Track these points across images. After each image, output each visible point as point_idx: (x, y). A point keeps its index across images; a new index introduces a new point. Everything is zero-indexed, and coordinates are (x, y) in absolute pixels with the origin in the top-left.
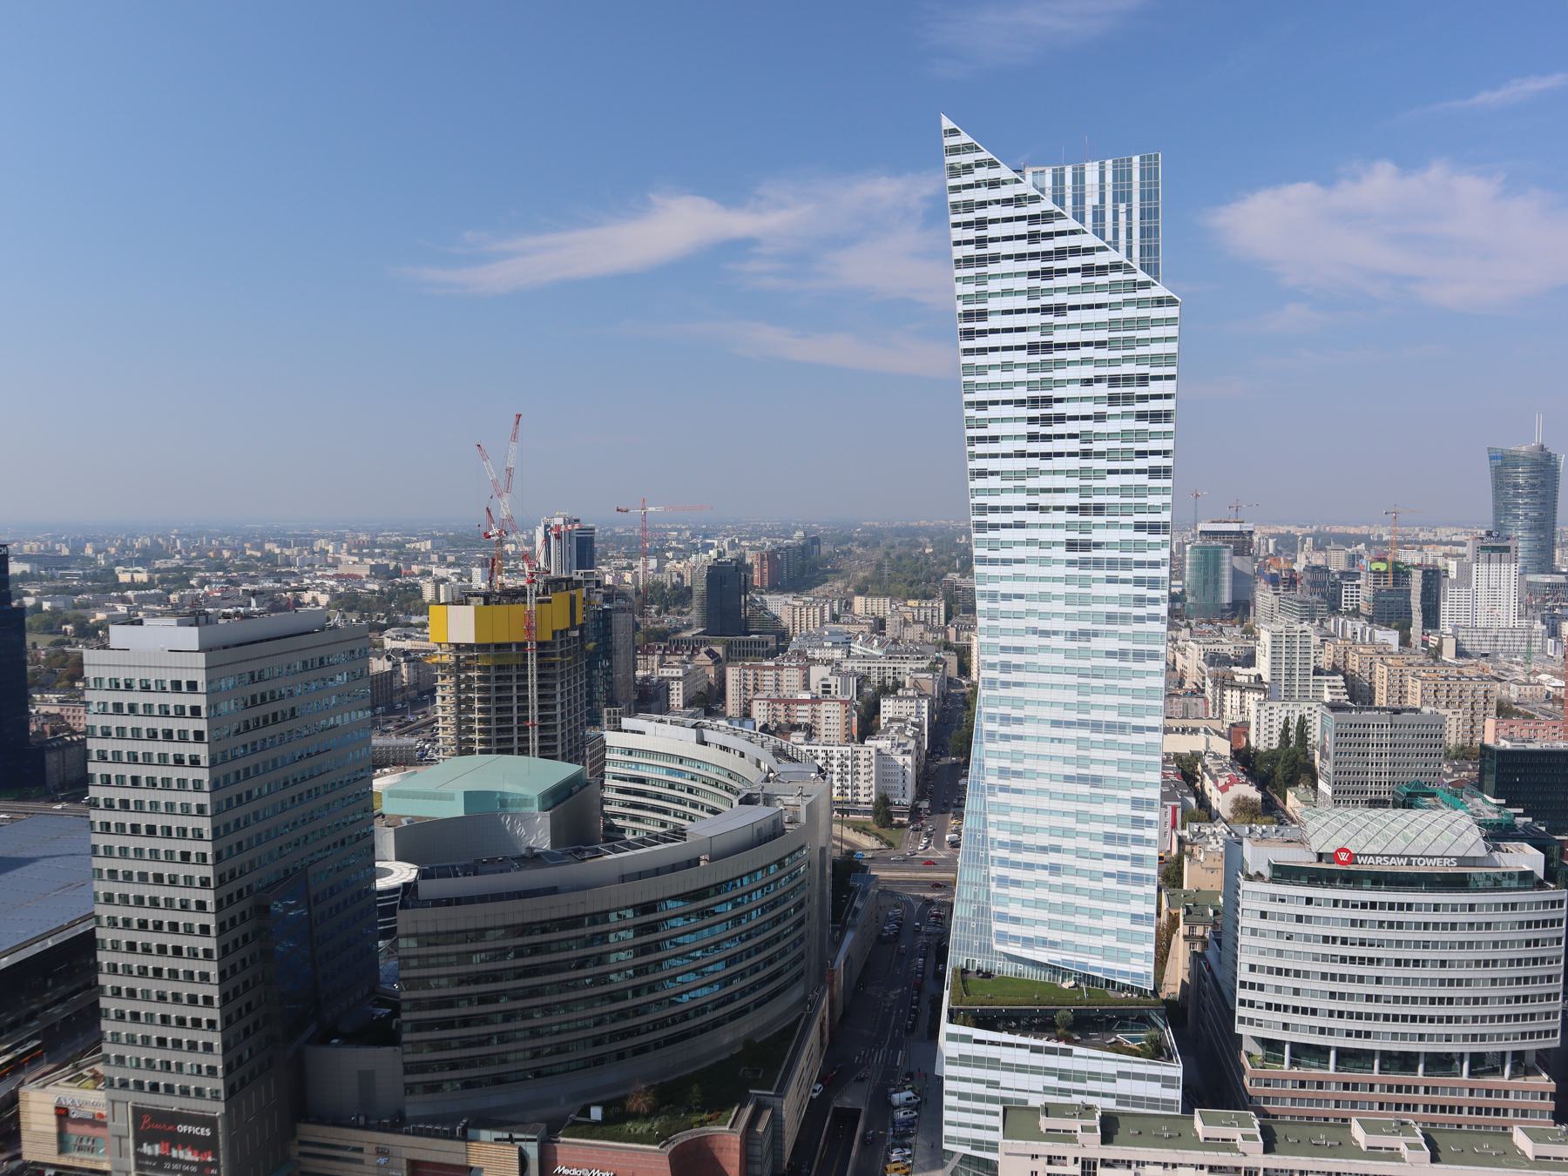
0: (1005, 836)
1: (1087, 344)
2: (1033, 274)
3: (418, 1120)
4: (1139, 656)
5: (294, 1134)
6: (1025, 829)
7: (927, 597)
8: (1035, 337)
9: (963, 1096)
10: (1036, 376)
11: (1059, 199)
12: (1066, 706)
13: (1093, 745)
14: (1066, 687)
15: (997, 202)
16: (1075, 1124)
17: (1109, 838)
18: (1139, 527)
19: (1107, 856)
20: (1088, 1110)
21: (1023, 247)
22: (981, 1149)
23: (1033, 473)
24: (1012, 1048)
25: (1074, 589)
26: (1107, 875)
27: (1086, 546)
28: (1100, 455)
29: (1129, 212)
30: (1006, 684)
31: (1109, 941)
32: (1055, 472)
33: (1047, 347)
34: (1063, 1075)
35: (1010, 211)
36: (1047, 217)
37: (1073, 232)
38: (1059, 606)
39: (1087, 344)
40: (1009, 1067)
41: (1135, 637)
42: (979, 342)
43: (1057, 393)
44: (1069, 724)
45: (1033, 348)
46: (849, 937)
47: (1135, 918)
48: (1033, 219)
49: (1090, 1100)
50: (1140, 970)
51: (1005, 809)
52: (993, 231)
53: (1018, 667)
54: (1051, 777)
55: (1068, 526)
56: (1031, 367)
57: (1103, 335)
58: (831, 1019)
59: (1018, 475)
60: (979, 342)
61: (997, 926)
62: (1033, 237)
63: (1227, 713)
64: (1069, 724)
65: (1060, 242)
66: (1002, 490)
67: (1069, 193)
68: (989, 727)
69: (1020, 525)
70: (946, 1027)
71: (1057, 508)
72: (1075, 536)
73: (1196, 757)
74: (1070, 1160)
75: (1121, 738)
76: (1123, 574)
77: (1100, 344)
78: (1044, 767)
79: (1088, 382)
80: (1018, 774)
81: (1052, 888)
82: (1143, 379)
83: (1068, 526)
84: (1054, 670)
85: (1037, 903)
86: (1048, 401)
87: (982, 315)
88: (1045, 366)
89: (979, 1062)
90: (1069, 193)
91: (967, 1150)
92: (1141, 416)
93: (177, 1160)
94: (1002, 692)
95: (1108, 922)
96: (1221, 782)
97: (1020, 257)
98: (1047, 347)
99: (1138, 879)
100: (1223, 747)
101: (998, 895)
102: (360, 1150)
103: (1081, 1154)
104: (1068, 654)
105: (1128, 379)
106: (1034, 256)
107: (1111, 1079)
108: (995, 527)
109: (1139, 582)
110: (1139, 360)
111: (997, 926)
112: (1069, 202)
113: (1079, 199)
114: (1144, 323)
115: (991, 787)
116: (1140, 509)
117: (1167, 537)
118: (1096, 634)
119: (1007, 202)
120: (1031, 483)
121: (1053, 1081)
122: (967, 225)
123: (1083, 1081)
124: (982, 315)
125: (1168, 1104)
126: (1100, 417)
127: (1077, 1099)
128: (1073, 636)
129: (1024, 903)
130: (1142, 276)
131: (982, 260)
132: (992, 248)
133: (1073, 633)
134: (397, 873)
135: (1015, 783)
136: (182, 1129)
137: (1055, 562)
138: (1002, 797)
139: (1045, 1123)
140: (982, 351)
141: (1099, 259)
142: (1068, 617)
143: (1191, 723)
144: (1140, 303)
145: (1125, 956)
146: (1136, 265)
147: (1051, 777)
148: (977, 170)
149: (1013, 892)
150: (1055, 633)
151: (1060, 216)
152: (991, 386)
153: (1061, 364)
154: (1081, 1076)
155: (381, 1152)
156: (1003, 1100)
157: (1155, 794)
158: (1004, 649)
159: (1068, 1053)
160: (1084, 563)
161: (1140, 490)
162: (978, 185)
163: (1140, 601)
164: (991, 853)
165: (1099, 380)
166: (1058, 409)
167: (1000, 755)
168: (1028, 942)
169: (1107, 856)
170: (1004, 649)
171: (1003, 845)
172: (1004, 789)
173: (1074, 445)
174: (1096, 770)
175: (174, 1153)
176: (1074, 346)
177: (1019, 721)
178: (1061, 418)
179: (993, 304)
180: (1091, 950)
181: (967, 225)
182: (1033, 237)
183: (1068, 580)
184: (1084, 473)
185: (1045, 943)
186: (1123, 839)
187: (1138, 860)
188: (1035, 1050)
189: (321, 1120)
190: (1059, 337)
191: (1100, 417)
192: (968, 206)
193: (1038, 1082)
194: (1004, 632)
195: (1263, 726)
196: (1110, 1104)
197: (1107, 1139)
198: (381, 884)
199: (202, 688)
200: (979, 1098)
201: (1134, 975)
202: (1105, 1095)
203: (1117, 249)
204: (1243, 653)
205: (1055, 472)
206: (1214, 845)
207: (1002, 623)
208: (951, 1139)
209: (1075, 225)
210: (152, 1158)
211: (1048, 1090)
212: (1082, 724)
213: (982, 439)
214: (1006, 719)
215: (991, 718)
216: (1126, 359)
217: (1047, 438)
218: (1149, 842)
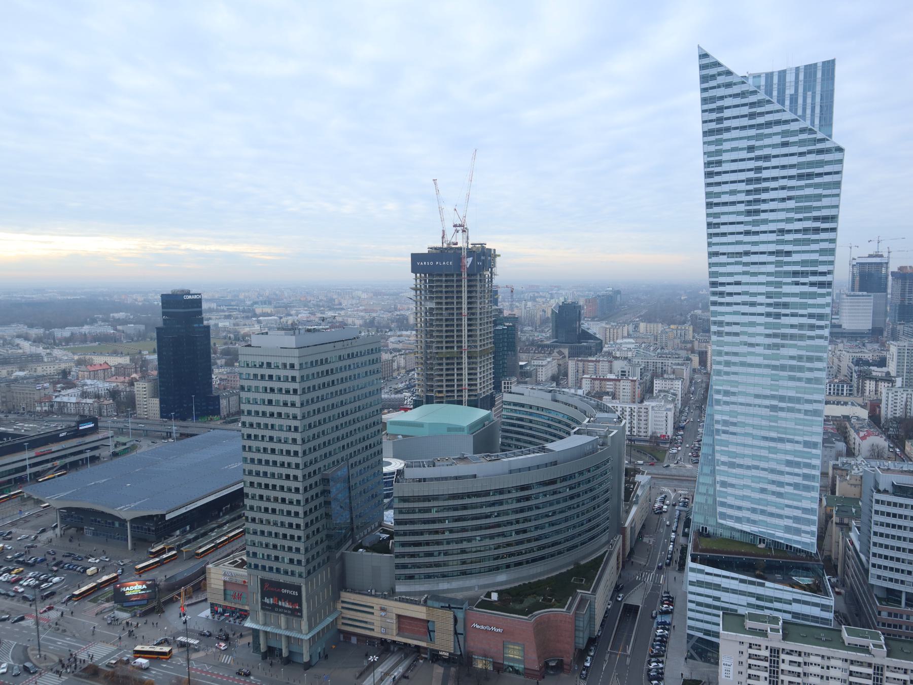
0: (724, 459)
1: (784, 178)
2: (749, 138)
3: (401, 593)
4: (810, 359)
5: (339, 597)
6: (736, 455)
7: (684, 323)
8: (751, 175)
9: (699, 604)
10: (751, 198)
11: (769, 92)
13: (782, 409)
14: (763, 376)
15: (730, 96)
16: (767, 627)
17: (789, 463)
18: (812, 284)
19: (788, 473)
20: (775, 620)
21: (745, 122)
22: (709, 635)
23: (747, 253)
24: (730, 580)
26: (789, 484)
29: (813, 98)
30: (727, 373)
31: (789, 523)
32: (762, 253)
33: (758, 180)
34: (759, 597)
35: (738, 101)
36: (760, 103)
37: (778, 111)
38: (761, 330)
39: (784, 178)
40: (726, 590)
41: (807, 348)
42: (717, 179)
43: (763, 207)
44: (766, 397)
45: (749, 181)
46: (634, 509)
47: (805, 510)
48: (752, 105)
49: (776, 614)
50: (808, 541)
51: (726, 443)
52: (727, 113)
53: (735, 364)
54: (753, 426)
55: (768, 284)
56: (748, 192)
57: (794, 172)
58: (623, 555)
59: (739, 254)
60: (717, 179)
61: (720, 509)
62: (752, 116)
63: (867, 393)
64: (766, 397)
65: (769, 118)
66: (729, 264)
67: (775, 87)
68: (716, 397)
69: (738, 283)
70: (690, 564)
71: (760, 273)
72: (771, 289)
73: (847, 418)
74: (763, 647)
75: (798, 406)
76: (801, 312)
77: (791, 177)
78: (750, 421)
79: (783, 200)
80: (734, 424)
82: (819, 197)
83: (768, 284)
84: (758, 366)
85: (743, 498)
86: (757, 212)
87: (719, 163)
88: (757, 191)
89: (708, 585)
90: (775, 87)
91: (701, 635)
92: (816, 219)
93: (281, 607)
94: (725, 378)
95: (787, 512)
96: (862, 434)
97: (743, 128)
98: (758, 180)
99: (807, 488)
100: (864, 414)
101: (720, 491)
102: (372, 607)
103: (770, 645)
104: (766, 357)
105: (808, 198)
106: (752, 127)
107: (789, 602)
108: (723, 284)
109: (811, 316)
110: (817, 186)
111: (720, 509)
112: (775, 93)
113: (782, 91)
114: (821, 163)
115: (718, 430)
116: (814, 273)
118: (783, 346)
119: (736, 96)
120: (745, 259)
121: (753, 601)
122: (711, 111)
123: (771, 602)
124: (719, 163)
125: (825, 621)
126: (789, 220)
127: (767, 612)
128: (769, 347)
129: (736, 497)
130: (820, 135)
131: (719, 131)
132: (726, 124)
133: (769, 345)
134: (394, 465)
135: (732, 429)
136: (284, 591)
137: (761, 304)
138: (724, 437)
139: (749, 624)
140: (719, 184)
141: (794, 126)
142: (768, 336)
143: (842, 399)
144: (820, 152)
145: (798, 532)
146: (816, 129)
147: (753, 426)
148: (718, 78)
149: (730, 490)
150: (758, 345)
151: (769, 102)
152: (725, 204)
153: (766, 190)
154: (771, 599)
155: (383, 609)
156: (723, 609)
157: (819, 439)
158: (727, 354)
159: (763, 585)
160: (777, 305)
161: (815, 263)
162: (719, 86)
163: (812, 327)
164: (717, 468)
165: (790, 198)
166: (763, 216)
167: (722, 413)
168: (738, 520)
169: (788, 473)
170: (727, 354)
171: (724, 463)
172: (725, 432)
173: (773, 237)
174: (783, 424)
175: (280, 603)
176: (775, 179)
177: (734, 394)
178: (765, 222)
179: (726, 157)
180: (776, 527)
181: (711, 111)
182: (752, 116)
183: (768, 315)
184: (778, 253)
185: (749, 521)
186: (798, 465)
187: (806, 477)
188: (742, 581)
189: (353, 591)
190: (765, 174)
191: (789, 220)
192: (713, 99)
193: (744, 600)
194: (728, 344)
195: (890, 402)
196: (788, 617)
197: (785, 637)
198: (386, 469)
199: (297, 367)
200: (708, 606)
202: (785, 612)
203: (805, 120)
204: (877, 359)
205: (762, 253)
206: (856, 471)
207: (727, 339)
208: (691, 628)
209: (778, 107)
210: (269, 605)
211: (750, 605)
212: (773, 397)
213: (717, 235)
214: (727, 393)
215: (718, 392)
216: (808, 186)
217: (757, 233)
218: (814, 467)
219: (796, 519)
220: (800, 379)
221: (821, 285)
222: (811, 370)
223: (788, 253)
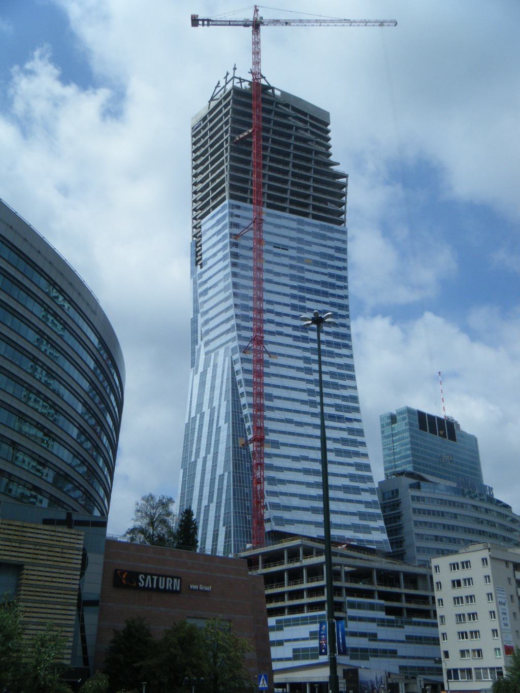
12: (299, 369)
18: (331, 276)
25: (296, 302)
27: (302, 279)
28: (308, 233)
104: (296, 338)
117: (345, 284)
128: (295, 328)
145: (367, 530)
160: (301, 289)
183: (293, 296)
184: (300, 240)
201: (377, 542)
219: (362, 515)
221: (340, 278)
222: (340, 356)
223: (309, 243)
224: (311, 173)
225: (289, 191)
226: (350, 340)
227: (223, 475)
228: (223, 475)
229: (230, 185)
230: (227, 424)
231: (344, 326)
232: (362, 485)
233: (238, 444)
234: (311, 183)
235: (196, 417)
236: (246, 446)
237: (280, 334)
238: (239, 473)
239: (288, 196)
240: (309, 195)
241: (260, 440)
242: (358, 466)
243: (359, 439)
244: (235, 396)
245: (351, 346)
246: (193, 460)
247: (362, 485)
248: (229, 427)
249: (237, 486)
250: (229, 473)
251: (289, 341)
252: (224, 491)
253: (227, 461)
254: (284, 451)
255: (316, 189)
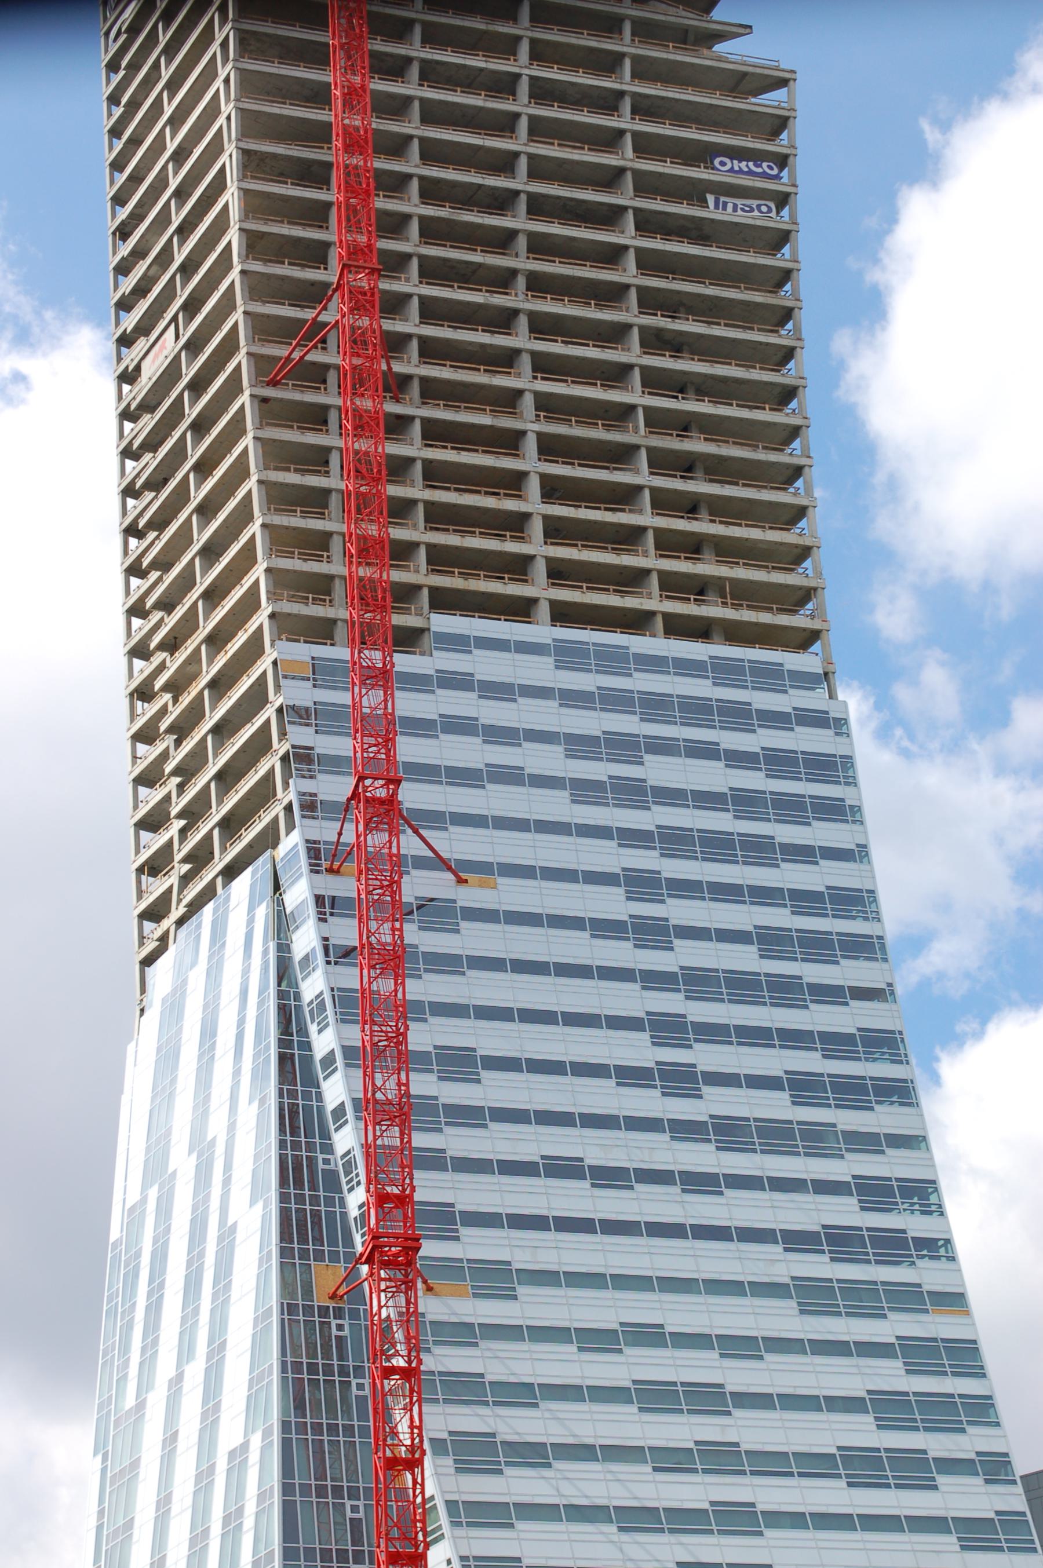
12: (605, 928)
17: (813, 1296)
81: (670, 1460)
104: (584, 791)
128: (579, 745)
142: (571, 698)
220: (763, 895)
224: (620, 79)
225: (523, 163)
226: (852, 782)
227: (245, 1447)
228: (245, 1447)
229: (246, 153)
230: (260, 1205)
231: (818, 720)
232: (938, 1445)
233: (308, 1292)
234: (624, 121)
235: (144, 1200)
236: (348, 1295)
237: (511, 776)
238: (317, 1428)
239: (519, 182)
240: (621, 171)
241: (397, 1256)
242: (918, 1354)
243: (916, 1225)
244: (294, 1067)
245: (856, 810)
246: (130, 1401)
247: (938, 1445)
248: (265, 1218)
249: (305, 1490)
250: (267, 1433)
251: (555, 805)
252: (249, 1522)
253: (260, 1377)
254: (536, 1306)
255: (645, 146)
